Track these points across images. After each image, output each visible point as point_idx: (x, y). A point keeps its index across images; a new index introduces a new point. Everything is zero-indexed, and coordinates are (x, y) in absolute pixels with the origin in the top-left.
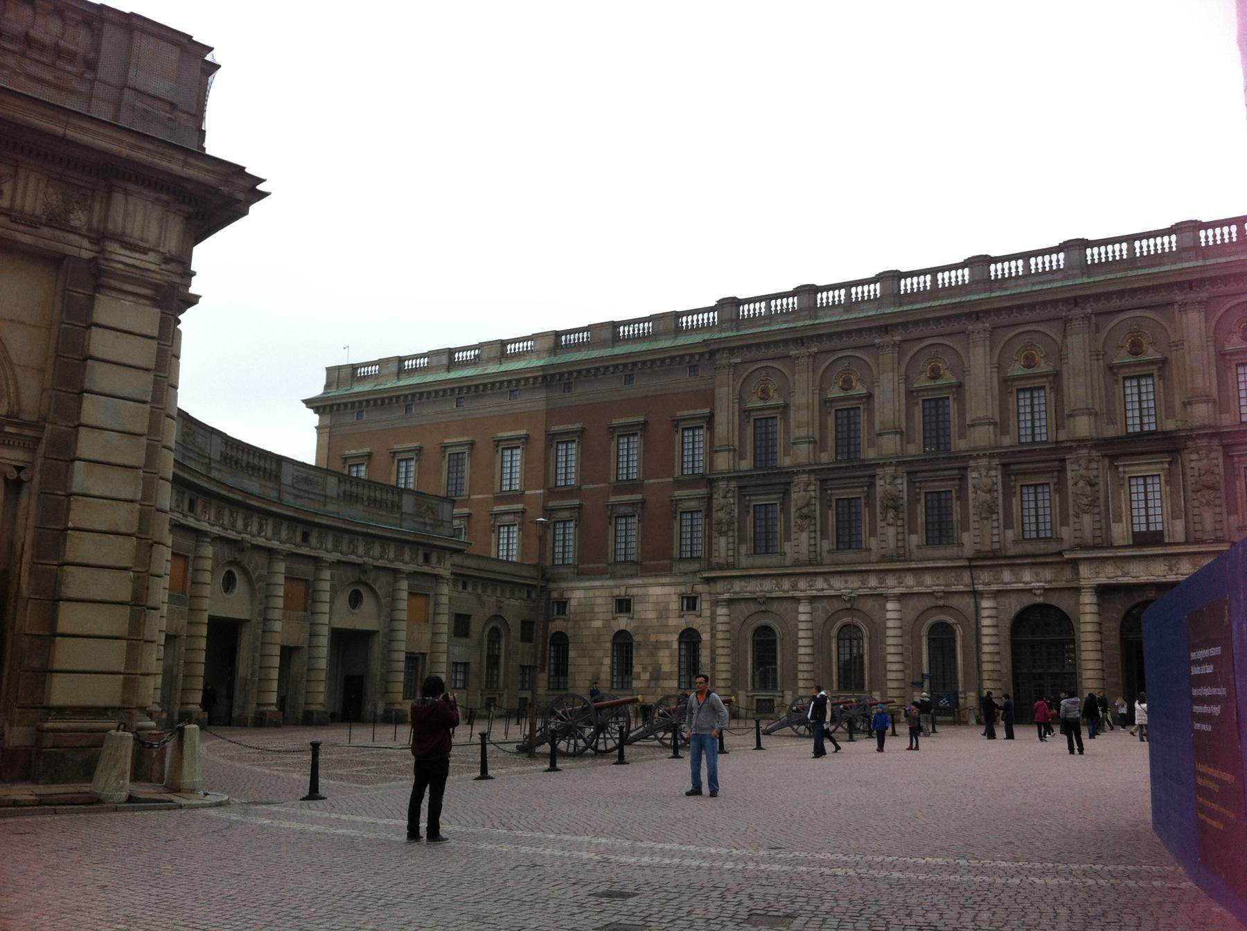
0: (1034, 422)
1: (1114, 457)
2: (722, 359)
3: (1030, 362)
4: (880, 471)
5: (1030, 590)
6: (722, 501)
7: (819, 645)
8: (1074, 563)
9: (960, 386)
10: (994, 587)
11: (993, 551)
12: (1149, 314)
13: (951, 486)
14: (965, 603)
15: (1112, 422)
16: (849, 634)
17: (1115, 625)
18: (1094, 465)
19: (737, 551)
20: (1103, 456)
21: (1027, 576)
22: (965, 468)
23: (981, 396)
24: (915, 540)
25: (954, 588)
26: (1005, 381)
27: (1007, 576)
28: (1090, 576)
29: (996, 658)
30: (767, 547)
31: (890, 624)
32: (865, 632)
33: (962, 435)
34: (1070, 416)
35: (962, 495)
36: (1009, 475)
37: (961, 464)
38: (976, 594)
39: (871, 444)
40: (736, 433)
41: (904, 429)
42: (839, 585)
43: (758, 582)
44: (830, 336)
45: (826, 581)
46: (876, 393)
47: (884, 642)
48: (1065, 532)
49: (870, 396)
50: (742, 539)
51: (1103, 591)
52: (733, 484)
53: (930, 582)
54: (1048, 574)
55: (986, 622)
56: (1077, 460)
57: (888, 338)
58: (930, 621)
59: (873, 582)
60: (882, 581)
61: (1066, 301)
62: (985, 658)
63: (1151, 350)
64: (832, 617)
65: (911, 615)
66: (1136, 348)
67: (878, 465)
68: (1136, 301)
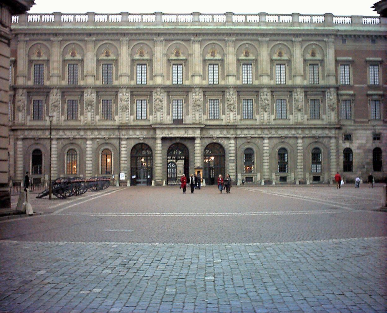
0: (142, 77)
1: (168, 92)
2: (21, 38)
3: (142, 54)
4: (85, 90)
5: (139, 138)
6: (20, 98)
7: (60, 157)
8: (155, 129)
9: (117, 60)
10: (126, 137)
11: (127, 123)
12: (182, 42)
13: (113, 98)
14: (115, 142)
15: (168, 79)
16: (72, 152)
17: (166, 151)
18: (162, 94)
19: (26, 118)
20: (165, 91)
21: (138, 133)
22: (117, 92)
23: (124, 67)
24: (98, 118)
25: (112, 136)
26: (133, 61)
27: (131, 132)
28: (160, 134)
29: (126, 162)
30: (38, 117)
31: (88, 149)
32: (78, 152)
33: (117, 79)
34: (154, 76)
35: (116, 102)
36: (133, 96)
37: (116, 90)
38: (120, 139)
39: (83, 79)
40: (27, 69)
41: (95, 74)
42: (69, 134)
43: (35, 131)
44: (67, 34)
45: (63, 132)
46: (85, 59)
47: (85, 156)
48: (151, 118)
49: (82, 60)
50: (28, 113)
51: (164, 139)
52: (25, 91)
53: (103, 134)
54: (145, 132)
55: (123, 149)
56: (156, 93)
57: (90, 38)
58: (102, 148)
59: (82, 133)
60: (85, 133)
61: (155, 34)
62: (122, 162)
63: (182, 55)
64: (64, 146)
65: (96, 146)
66: (177, 55)
67: (85, 88)
68: (178, 37)
